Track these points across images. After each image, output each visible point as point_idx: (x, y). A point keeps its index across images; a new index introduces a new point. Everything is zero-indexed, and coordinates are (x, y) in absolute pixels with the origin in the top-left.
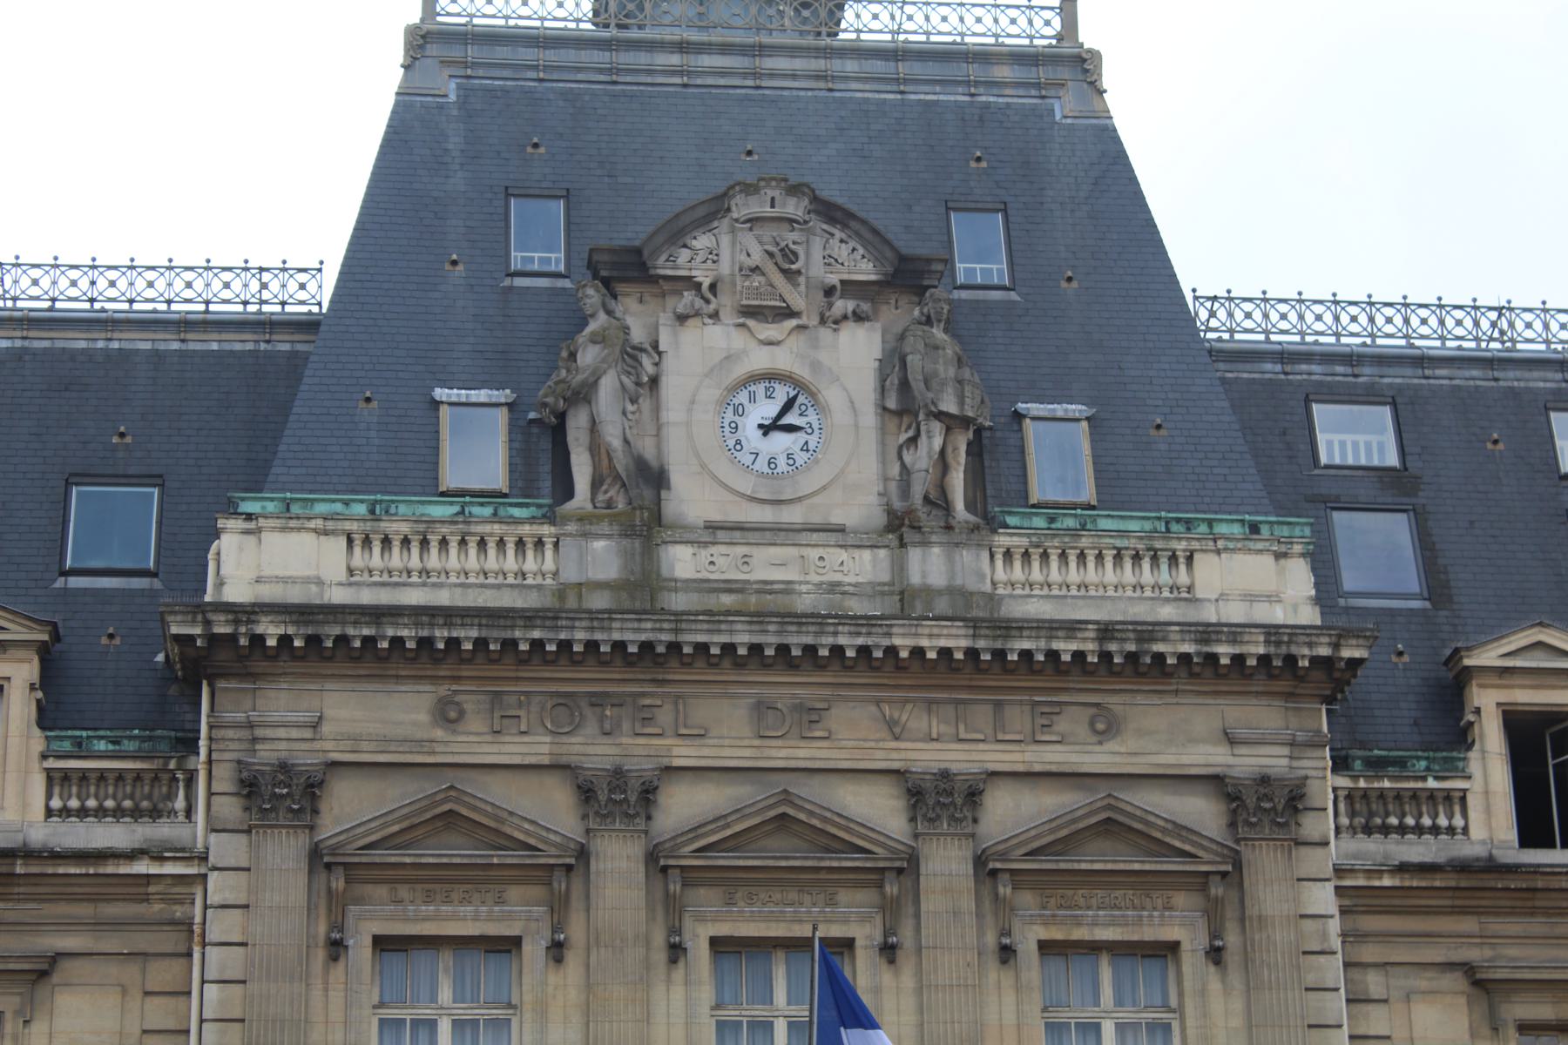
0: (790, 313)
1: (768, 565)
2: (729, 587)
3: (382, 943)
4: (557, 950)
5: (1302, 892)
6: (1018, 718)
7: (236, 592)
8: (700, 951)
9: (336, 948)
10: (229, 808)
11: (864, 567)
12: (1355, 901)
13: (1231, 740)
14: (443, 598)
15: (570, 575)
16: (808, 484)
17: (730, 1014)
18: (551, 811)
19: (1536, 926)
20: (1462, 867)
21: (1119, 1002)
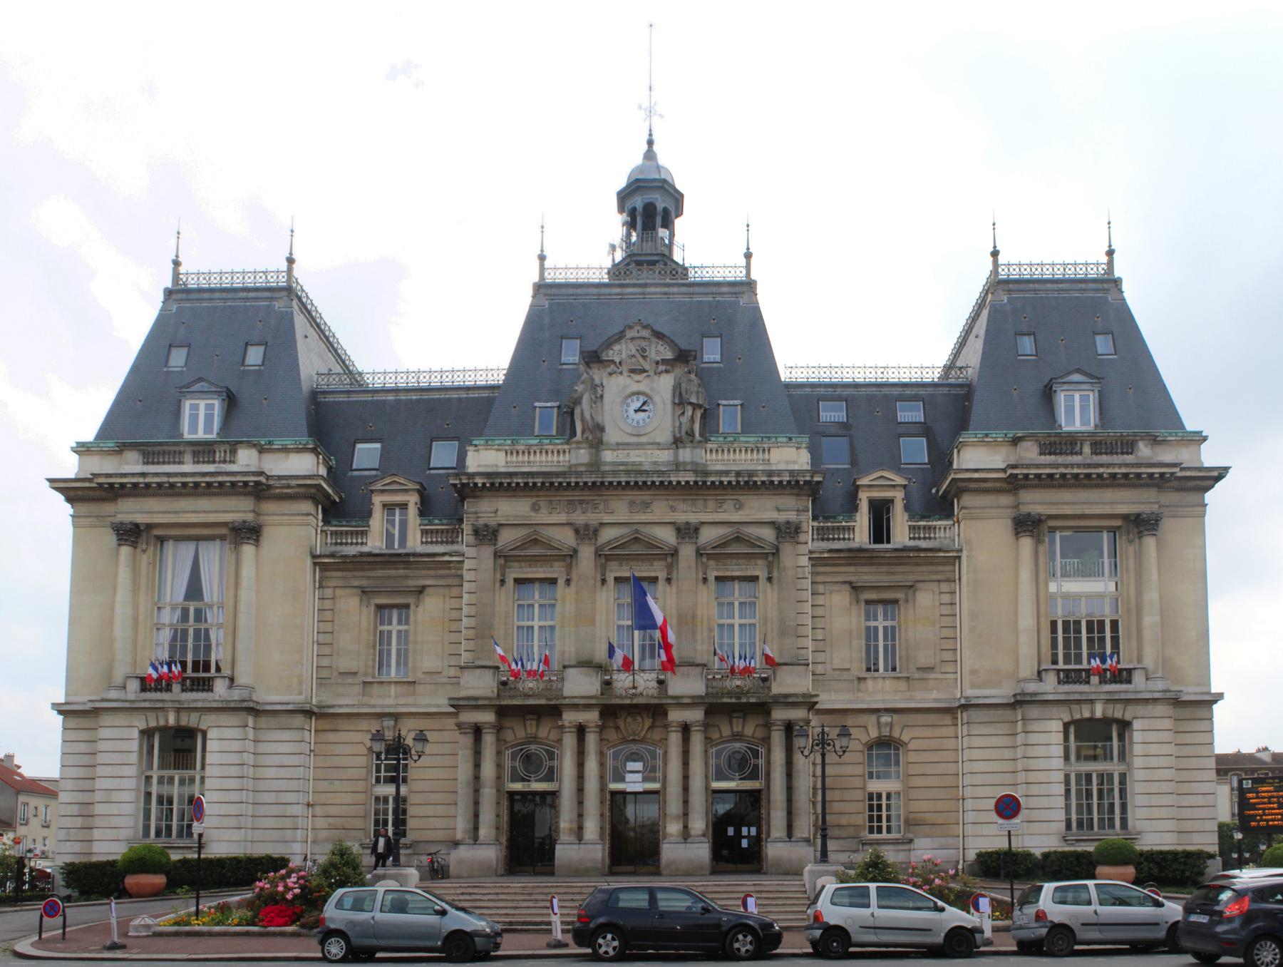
0: (645, 371)
1: (635, 456)
2: (623, 464)
3: (516, 580)
4: (568, 582)
5: (797, 559)
6: (711, 504)
7: (471, 469)
8: (611, 581)
9: (503, 582)
10: (471, 539)
11: (665, 456)
12: (816, 561)
13: (779, 510)
14: (534, 469)
15: (573, 462)
16: (649, 429)
17: (621, 601)
18: (566, 538)
19: (873, 569)
20: (850, 550)
21: (741, 595)
